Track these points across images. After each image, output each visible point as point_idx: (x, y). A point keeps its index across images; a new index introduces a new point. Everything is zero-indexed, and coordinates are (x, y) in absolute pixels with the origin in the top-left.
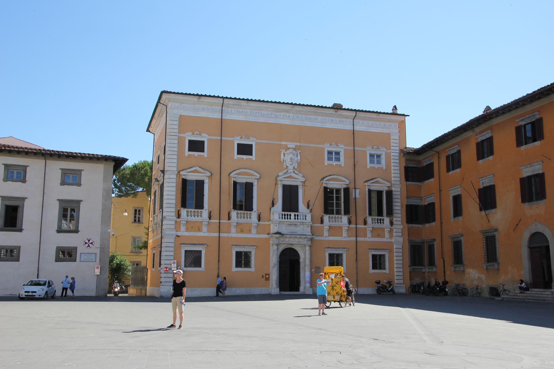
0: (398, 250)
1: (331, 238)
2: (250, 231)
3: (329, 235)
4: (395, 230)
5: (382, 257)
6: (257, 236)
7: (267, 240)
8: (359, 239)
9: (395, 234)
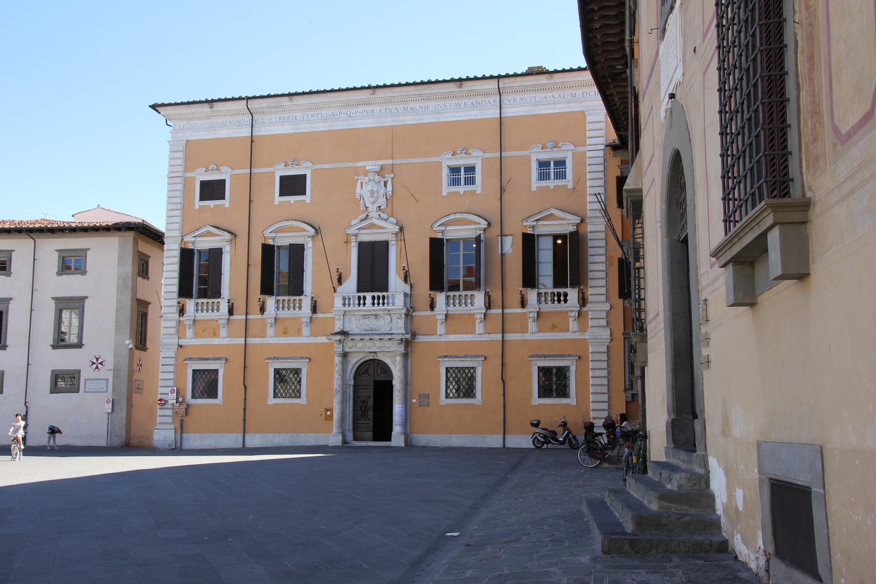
0: (597, 357)
1: (452, 338)
2: (299, 333)
3: (448, 333)
4: (590, 315)
5: (562, 372)
6: (312, 340)
7: (330, 346)
8: (509, 337)
9: (590, 323)
